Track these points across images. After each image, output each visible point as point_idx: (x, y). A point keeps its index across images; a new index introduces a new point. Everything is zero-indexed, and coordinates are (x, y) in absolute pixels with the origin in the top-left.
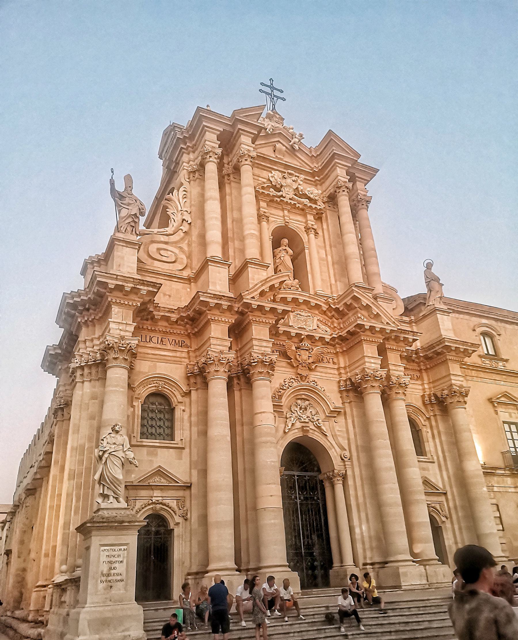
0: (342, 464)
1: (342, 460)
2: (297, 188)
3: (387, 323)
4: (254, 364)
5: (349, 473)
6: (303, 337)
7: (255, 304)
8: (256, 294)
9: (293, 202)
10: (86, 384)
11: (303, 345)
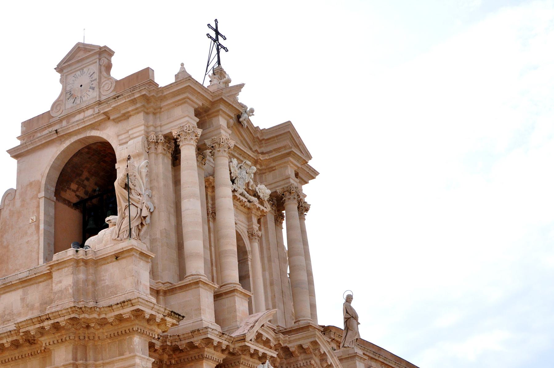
9: (244, 200)
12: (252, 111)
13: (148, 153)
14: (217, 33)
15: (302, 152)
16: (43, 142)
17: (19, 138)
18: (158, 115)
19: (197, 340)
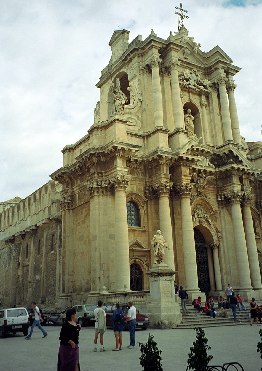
0: (217, 240)
1: (218, 237)
2: (197, 79)
3: (246, 166)
4: (183, 189)
5: (221, 245)
6: (201, 171)
7: (185, 157)
8: (185, 151)
9: (195, 88)
10: (100, 197)
11: (202, 175)
12: (199, 45)
13: (140, 74)
14: (182, 10)
15: (227, 60)
16: (106, 79)
17: (100, 79)
18: (144, 56)
19: (155, 157)
